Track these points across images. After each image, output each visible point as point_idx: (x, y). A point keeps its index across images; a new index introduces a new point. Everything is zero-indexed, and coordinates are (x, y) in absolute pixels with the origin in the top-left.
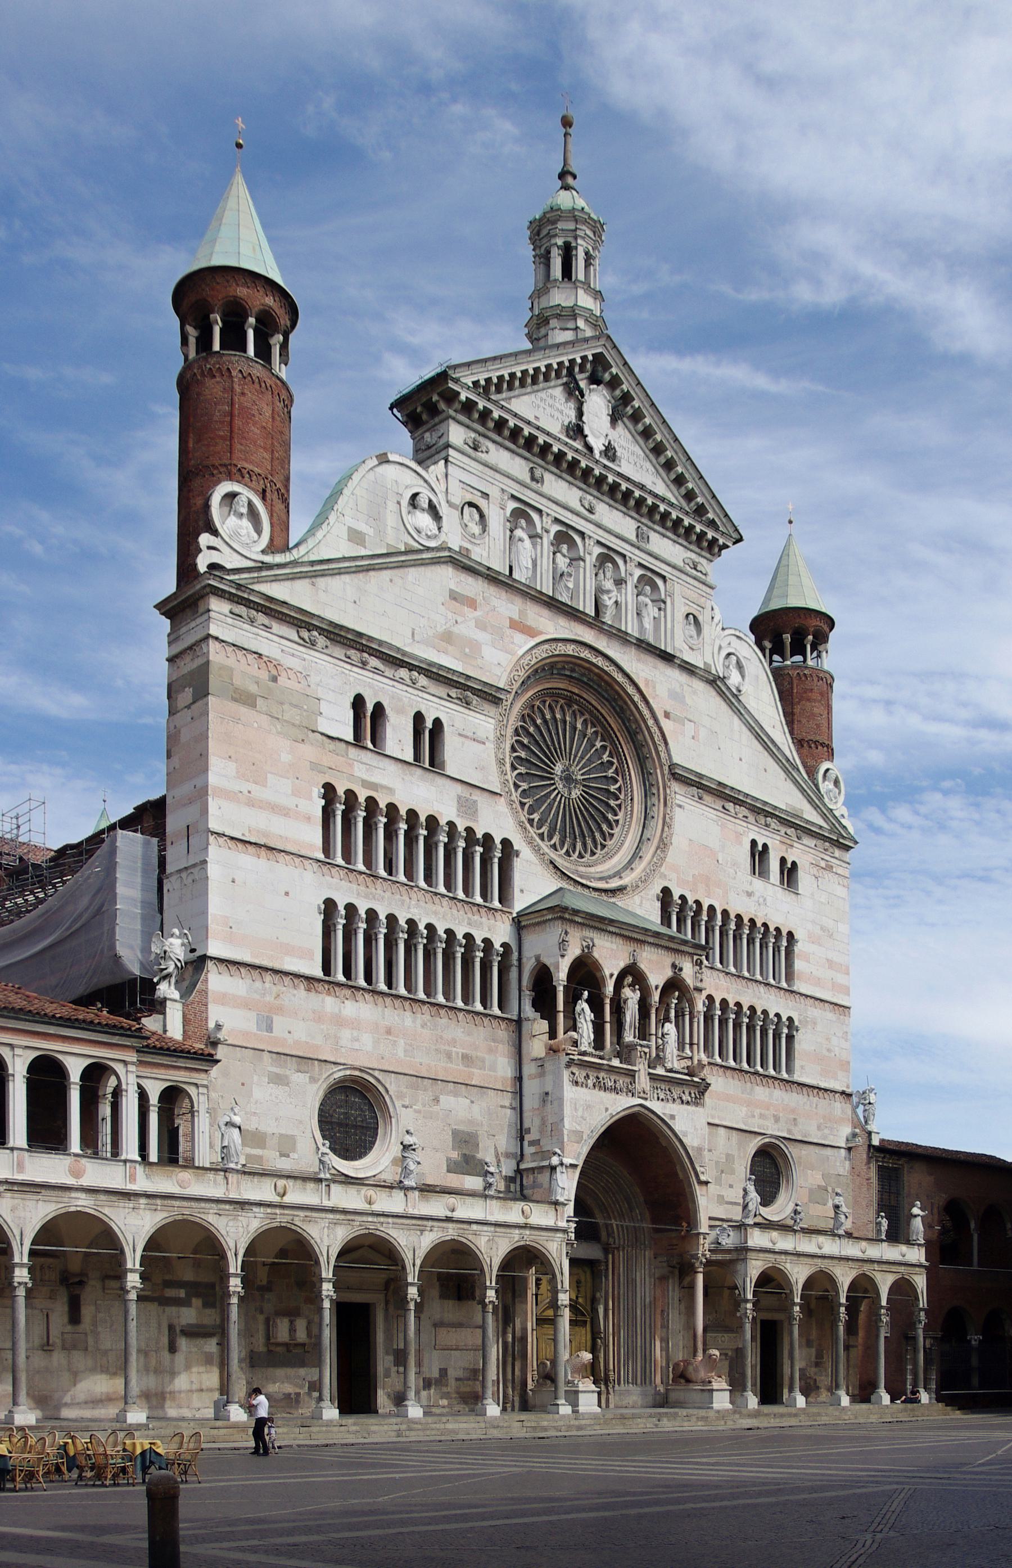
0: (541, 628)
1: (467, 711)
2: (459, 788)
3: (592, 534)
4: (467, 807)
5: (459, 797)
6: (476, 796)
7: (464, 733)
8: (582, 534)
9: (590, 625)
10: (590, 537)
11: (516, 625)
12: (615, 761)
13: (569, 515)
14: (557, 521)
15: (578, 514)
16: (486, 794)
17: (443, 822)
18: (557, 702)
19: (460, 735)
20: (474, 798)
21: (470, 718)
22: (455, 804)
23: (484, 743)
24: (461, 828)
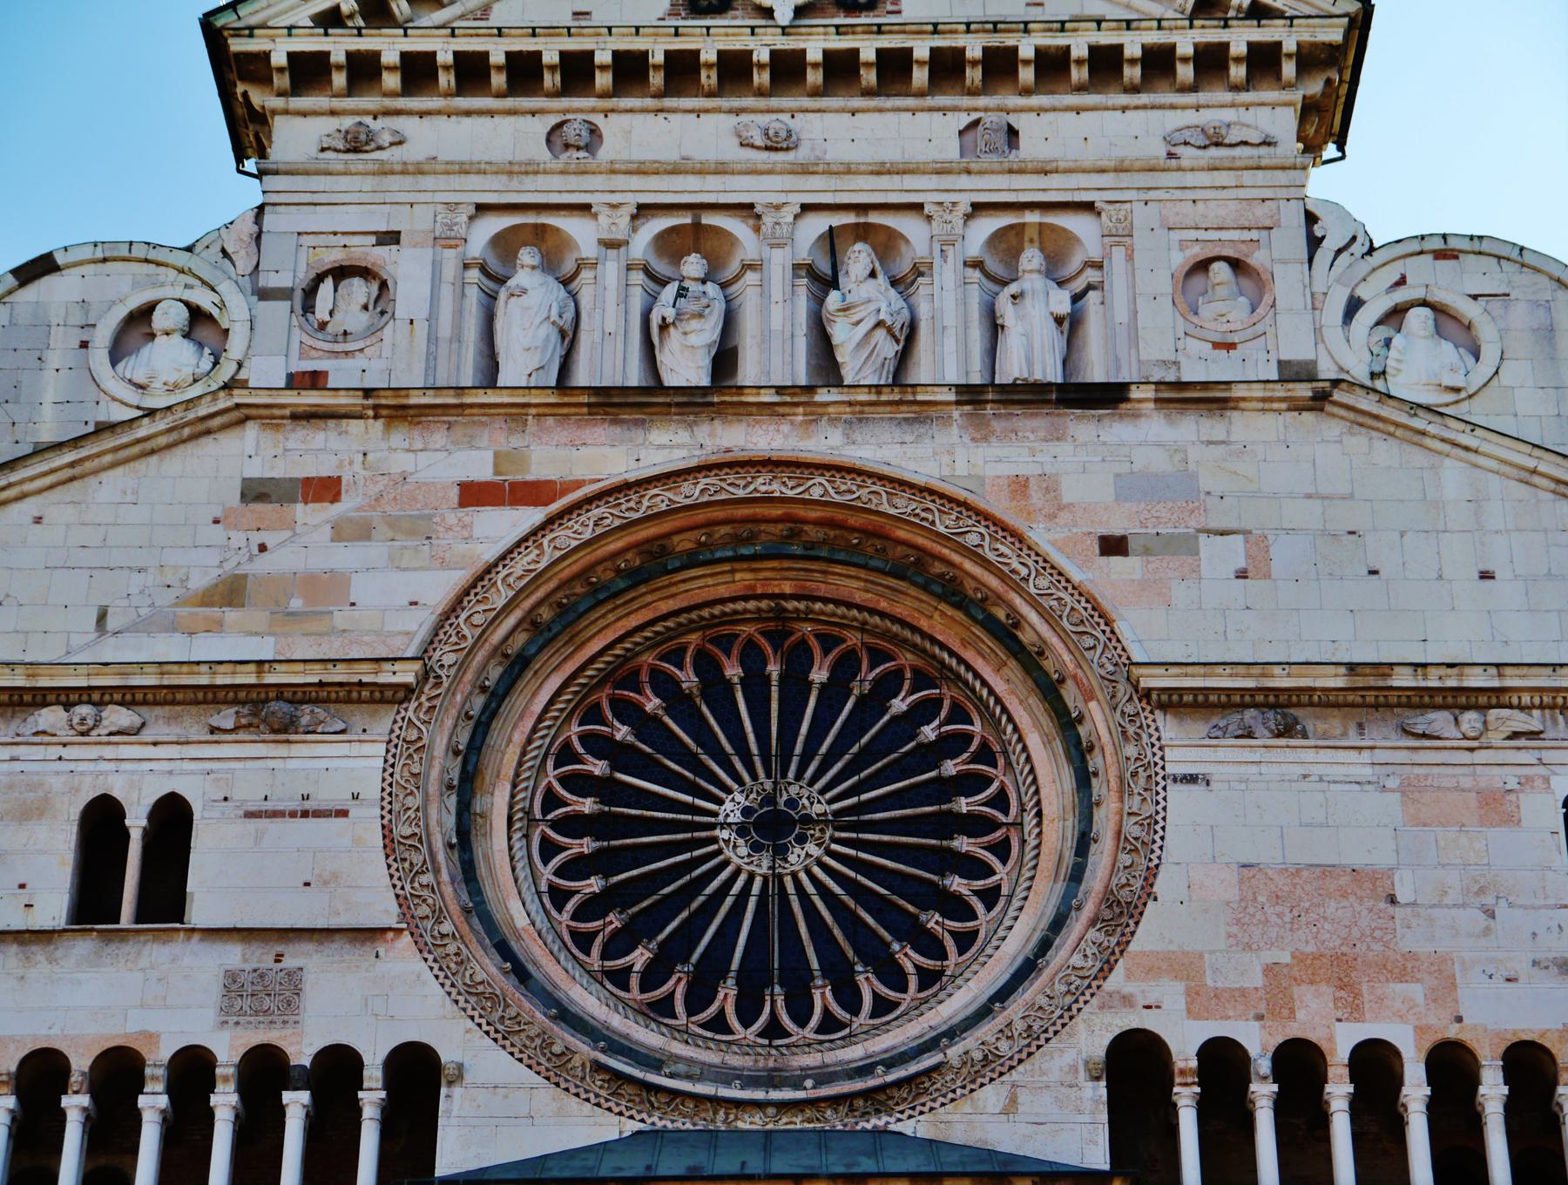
0: (579, 473)
1: (281, 750)
2: (233, 955)
3: (781, 198)
4: (239, 993)
5: (232, 977)
6: (298, 956)
7: (269, 806)
8: (745, 209)
9: (717, 411)
10: (778, 207)
11: (474, 494)
12: (446, 684)
13: (692, 182)
14: (644, 210)
15: (721, 169)
16: (336, 946)
17: (158, 1056)
18: (683, 649)
19: (250, 815)
20: (289, 963)
21: (292, 764)
22: (216, 991)
23: (343, 813)
24: (228, 1050)
